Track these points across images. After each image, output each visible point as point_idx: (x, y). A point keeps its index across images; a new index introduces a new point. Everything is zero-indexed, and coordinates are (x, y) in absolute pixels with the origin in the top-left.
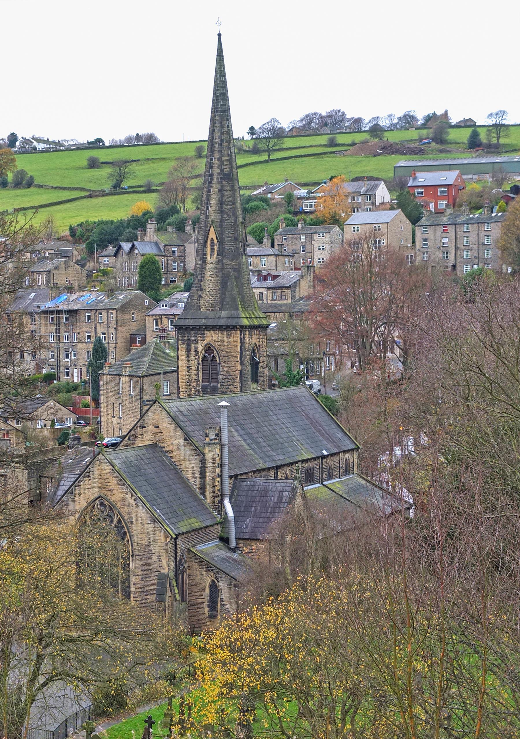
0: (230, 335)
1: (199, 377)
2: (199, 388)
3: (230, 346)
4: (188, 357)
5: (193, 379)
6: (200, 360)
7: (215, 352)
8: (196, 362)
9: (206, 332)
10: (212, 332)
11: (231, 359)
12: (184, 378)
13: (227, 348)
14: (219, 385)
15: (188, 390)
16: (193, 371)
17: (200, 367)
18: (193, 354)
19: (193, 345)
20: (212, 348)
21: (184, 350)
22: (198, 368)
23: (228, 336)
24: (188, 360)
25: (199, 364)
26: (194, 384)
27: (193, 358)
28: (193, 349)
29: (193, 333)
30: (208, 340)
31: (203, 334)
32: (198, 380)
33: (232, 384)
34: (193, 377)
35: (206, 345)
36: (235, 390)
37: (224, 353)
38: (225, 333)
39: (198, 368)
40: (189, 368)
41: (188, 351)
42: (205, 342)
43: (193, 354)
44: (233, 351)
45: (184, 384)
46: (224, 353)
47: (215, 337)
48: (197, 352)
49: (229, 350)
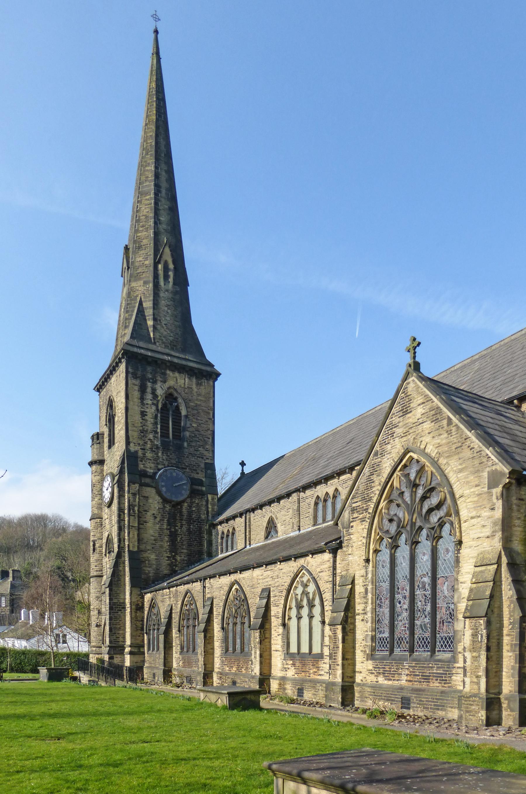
0: (201, 384)
1: (157, 428)
2: (158, 443)
3: (200, 398)
4: (142, 399)
5: (149, 429)
6: (160, 406)
7: (180, 400)
8: (154, 408)
9: (168, 372)
10: (177, 374)
11: (202, 414)
12: (136, 425)
13: (197, 400)
14: (185, 444)
15: (141, 442)
16: (149, 418)
17: (159, 415)
18: (149, 396)
19: (149, 384)
20: (176, 395)
21: (136, 388)
22: (156, 416)
23: (198, 384)
24: (143, 404)
25: (157, 410)
26: (151, 436)
27: (150, 402)
28: (149, 390)
29: (149, 369)
30: (171, 383)
31: (164, 374)
32: (156, 432)
33: (203, 446)
34: (150, 426)
35: (169, 388)
36: (206, 453)
37: (192, 404)
38: (194, 380)
39: (156, 416)
40: (143, 414)
41: (143, 390)
42: (167, 385)
43: (149, 396)
44: (203, 404)
45: (136, 434)
46: (192, 404)
47: (181, 382)
48: (155, 396)
49: (199, 403)
